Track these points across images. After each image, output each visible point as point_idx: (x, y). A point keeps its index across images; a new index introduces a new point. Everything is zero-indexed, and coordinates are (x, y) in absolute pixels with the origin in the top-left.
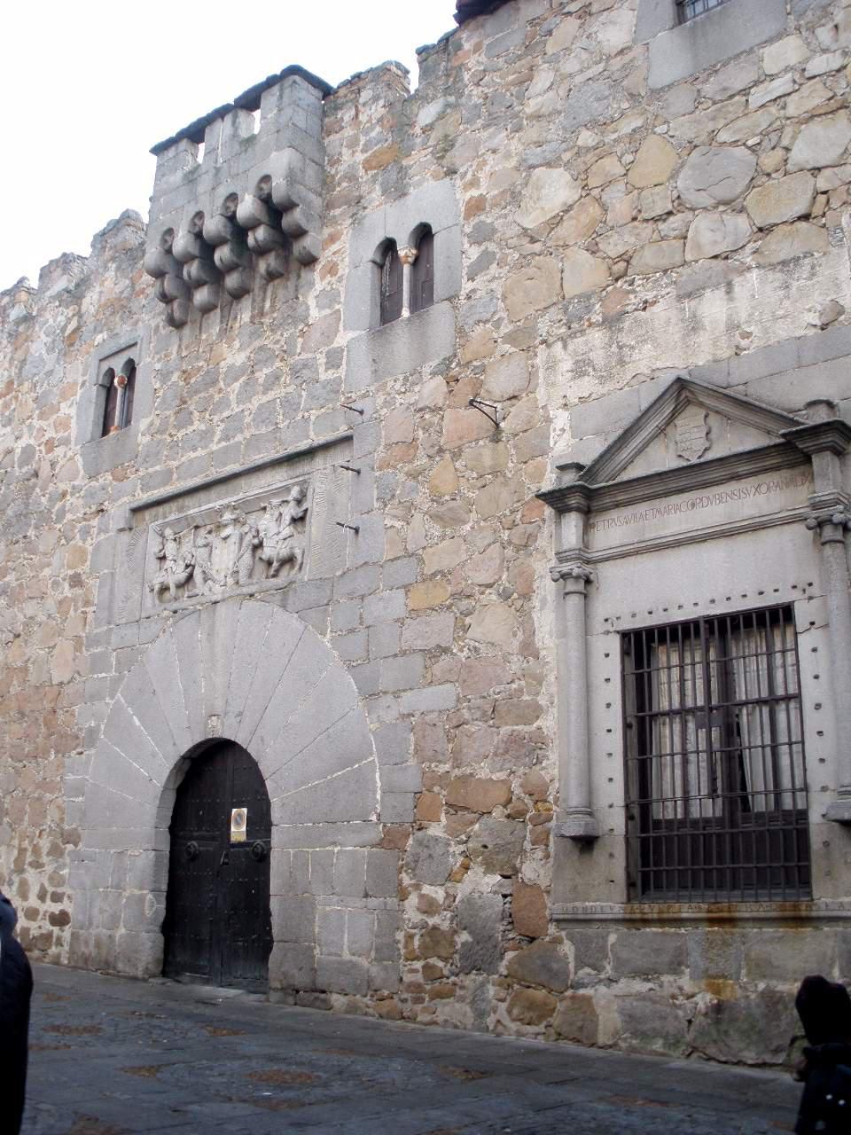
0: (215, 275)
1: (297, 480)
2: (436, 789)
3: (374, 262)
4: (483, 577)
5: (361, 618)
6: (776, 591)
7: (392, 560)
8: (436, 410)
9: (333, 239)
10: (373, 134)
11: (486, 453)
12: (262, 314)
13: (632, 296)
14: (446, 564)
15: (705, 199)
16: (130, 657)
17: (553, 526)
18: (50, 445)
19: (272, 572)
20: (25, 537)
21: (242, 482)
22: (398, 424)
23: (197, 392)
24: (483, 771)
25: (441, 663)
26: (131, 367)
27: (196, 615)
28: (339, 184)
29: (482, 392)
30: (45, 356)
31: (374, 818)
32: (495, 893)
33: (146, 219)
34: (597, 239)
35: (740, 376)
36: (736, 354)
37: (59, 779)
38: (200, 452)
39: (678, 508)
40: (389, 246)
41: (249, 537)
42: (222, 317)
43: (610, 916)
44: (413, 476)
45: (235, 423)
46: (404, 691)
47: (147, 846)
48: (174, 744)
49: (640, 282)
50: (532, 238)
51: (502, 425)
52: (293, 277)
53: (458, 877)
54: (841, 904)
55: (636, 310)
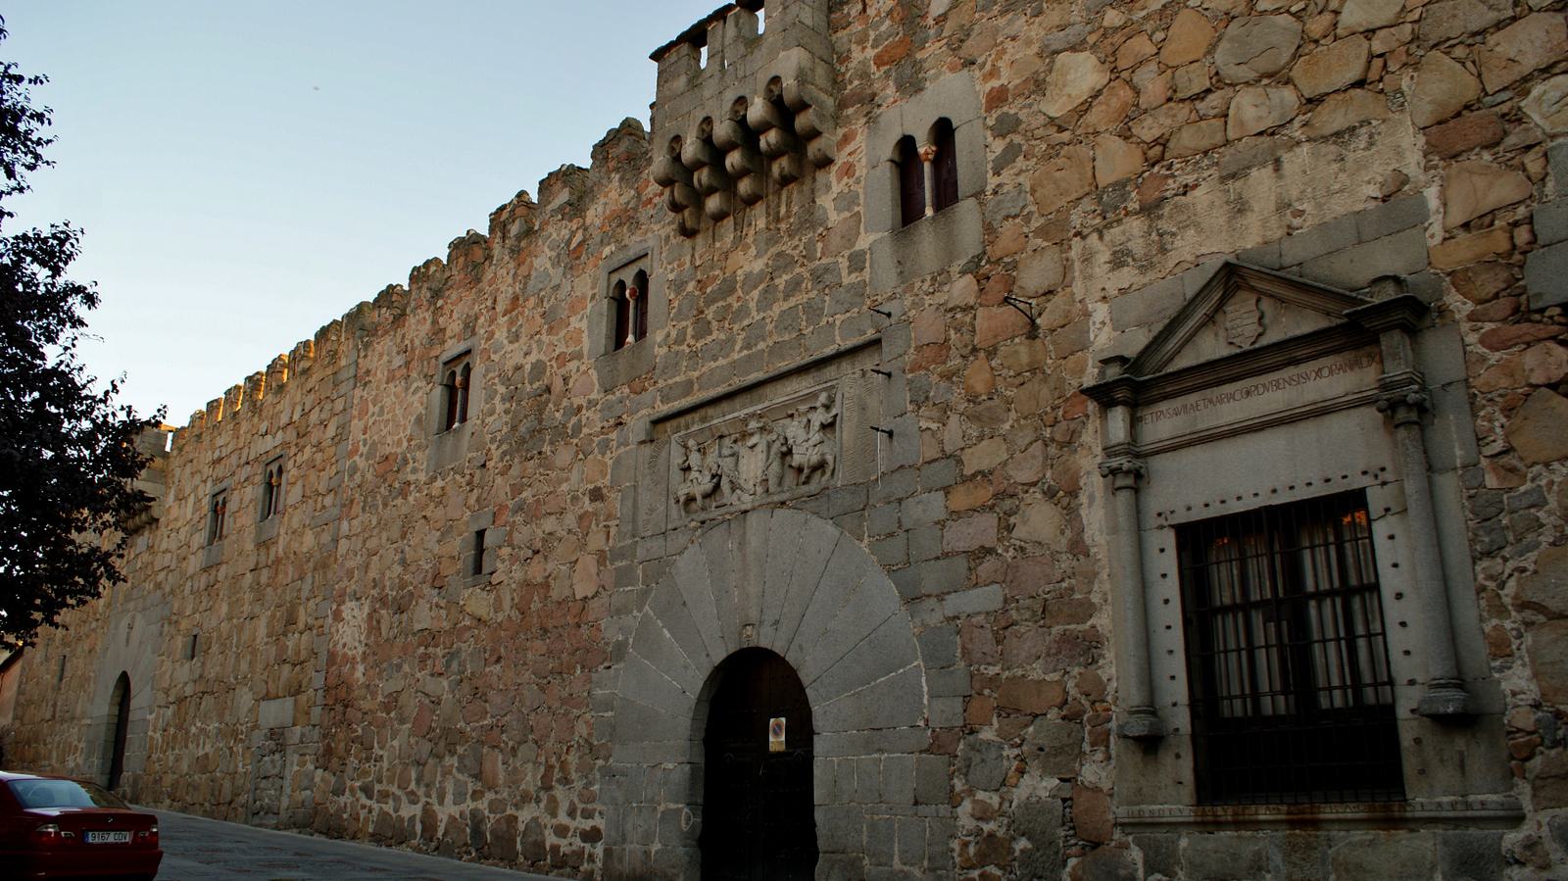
0: (727, 182)
1: (825, 385)
2: (986, 692)
3: (892, 161)
4: (1024, 475)
5: (899, 521)
6: (1345, 477)
7: (929, 463)
8: (967, 309)
9: (846, 139)
10: (883, 28)
11: (1023, 351)
12: (778, 220)
13: (1170, 181)
14: (985, 465)
15: (1246, 73)
16: (660, 568)
17: (1098, 421)
18: (563, 360)
19: (803, 478)
20: (540, 453)
21: (768, 390)
22: (928, 326)
23: (714, 301)
24: (1036, 671)
25: (986, 565)
26: (642, 278)
27: (725, 525)
28: (851, 82)
29: (1016, 289)
30: (551, 271)
31: (922, 723)
32: (1054, 797)
33: (647, 128)
34: (1130, 124)
35: (1293, 253)
36: (1289, 234)
37: (586, 694)
38: (722, 362)
39: (1232, 397)
40: (907, 144)
41: (777, 445)
42: (735, 224)
43: (1180, 819)
44: (948, 377)
45: (755, 333)
46: (949, 593)
47: (680, 760)
48: (708, 655)
49: (1179, 166)
50: (1059, 127)
51: (1038, 321)
52: (808, 180)
53: (1014, 781)
54: (1439, 804)
55: (1176, 195)
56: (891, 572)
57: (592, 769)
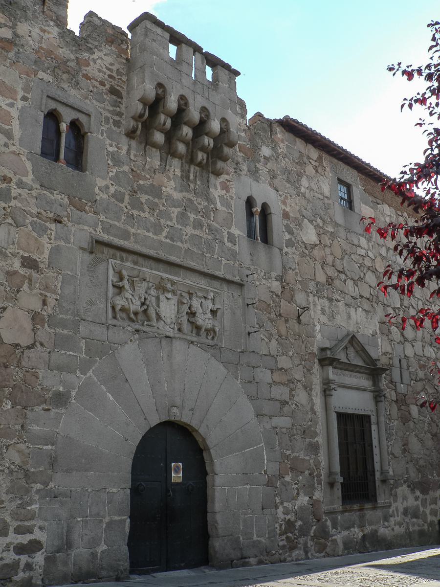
0: (171, 135)
1: (214, 290)
2: (286, 461)
21: (182, 272)
31: (263, 473)
37: (18, 427)
46: (274, 416)
47: (124, 486)
48: (145, 419)
56: (250, 398)
57: (28, 491)
